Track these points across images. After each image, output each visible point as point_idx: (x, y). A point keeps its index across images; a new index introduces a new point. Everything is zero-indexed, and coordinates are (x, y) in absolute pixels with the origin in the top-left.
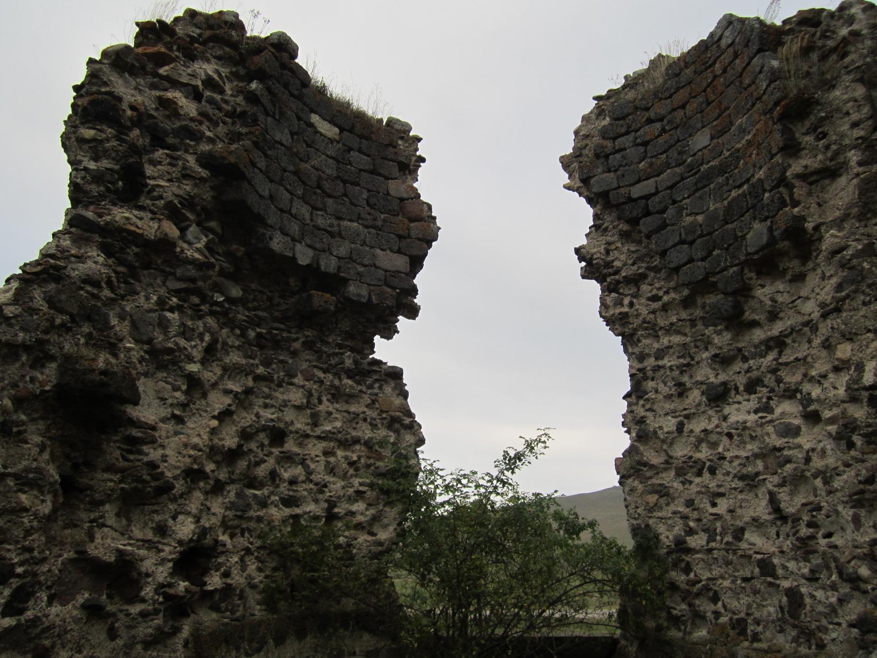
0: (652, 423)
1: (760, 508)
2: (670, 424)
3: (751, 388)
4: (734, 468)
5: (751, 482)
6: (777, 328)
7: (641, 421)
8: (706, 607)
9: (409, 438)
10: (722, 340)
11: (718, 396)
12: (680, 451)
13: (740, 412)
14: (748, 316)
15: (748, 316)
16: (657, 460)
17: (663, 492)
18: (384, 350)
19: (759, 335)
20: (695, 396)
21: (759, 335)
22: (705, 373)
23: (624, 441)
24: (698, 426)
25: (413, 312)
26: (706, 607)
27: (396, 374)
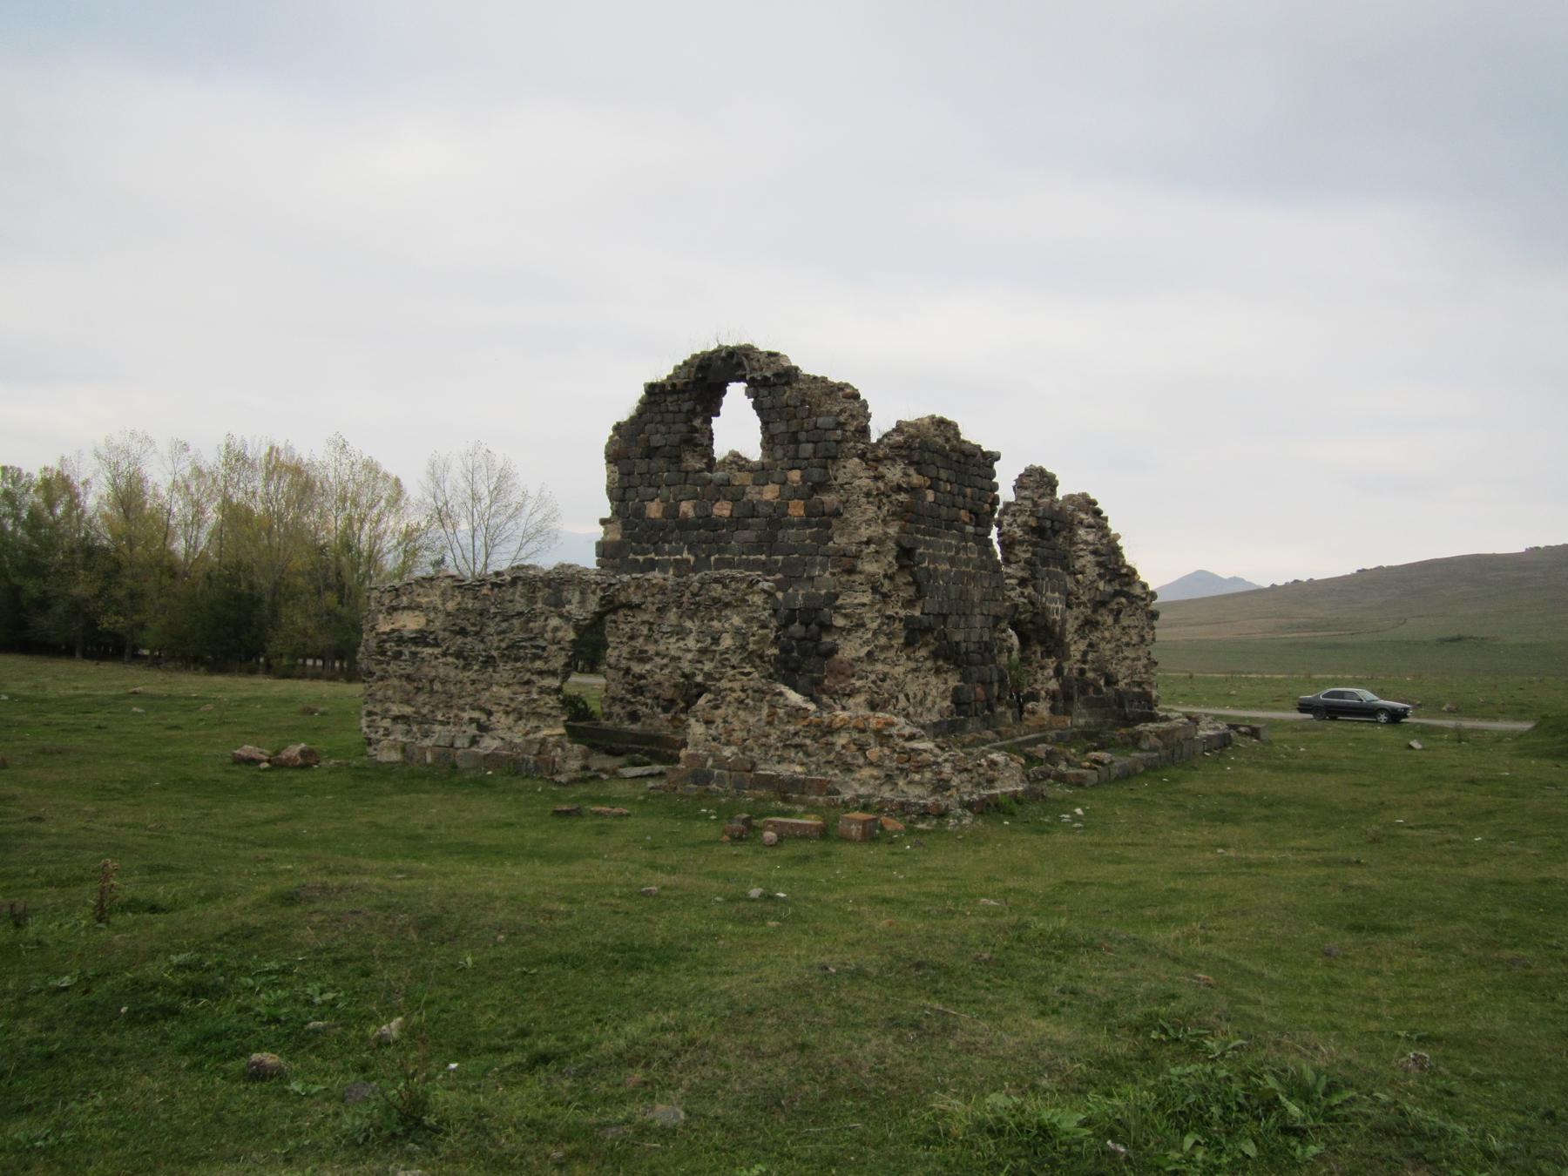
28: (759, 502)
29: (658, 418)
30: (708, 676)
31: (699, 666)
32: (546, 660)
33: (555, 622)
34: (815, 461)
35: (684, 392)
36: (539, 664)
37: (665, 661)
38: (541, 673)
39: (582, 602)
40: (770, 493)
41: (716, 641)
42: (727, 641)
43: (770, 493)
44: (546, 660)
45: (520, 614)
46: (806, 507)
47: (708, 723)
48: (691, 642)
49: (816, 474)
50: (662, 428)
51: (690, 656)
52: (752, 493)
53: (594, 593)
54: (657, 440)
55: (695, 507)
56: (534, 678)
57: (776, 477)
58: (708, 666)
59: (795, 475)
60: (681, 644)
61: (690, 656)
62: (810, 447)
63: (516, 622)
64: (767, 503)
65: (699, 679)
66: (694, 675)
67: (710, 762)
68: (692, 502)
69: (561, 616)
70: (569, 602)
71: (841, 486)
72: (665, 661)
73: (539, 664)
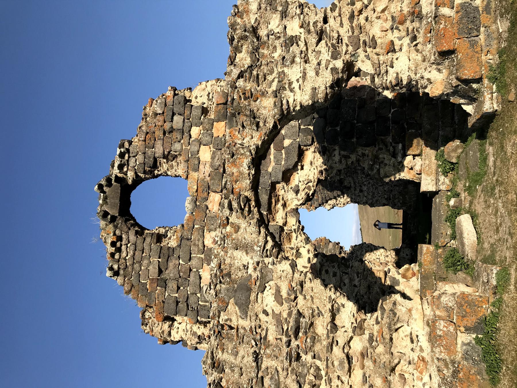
0: (364, 201)
1: (381, 188)
2: (365, 198)
3: (361, 186)
4: (374, 190)
5: (376, 188)
6: (352, 182)
7: (364, 203)
8: (397, 196)
9: (365, 245)
10: (352, 189)
11: (361, 191)
12: (370, 197)
13: (365, 188)
14: (349, 186)
15: (349, 186)
16: (371, 201)
17: (377, 201)
18: (347, 248)
19: (352, 185)
20: (360, 194)
21: (352, 185)
22: (357, 192)
23: (368, 207)
24: (366, 194)
25: (339, 243)
26: (397, 196)
27: (352, 247)
28: (212, 166)
29: (136, 266)
30: (335, 56)
31: (323, 63)
32: (316, 313)
33: (268, 299)
34: (187, 112)
35: (120, 238)
36: (321, 327)
37: (347, 281)
38: (334, 327)
39: (247, 248)
40: (205, 154)
41: (293, 40)
42: (294, 28)
43: (205, 154)
44: (316, 313)
45: (257, 357)
46: (218, 121)
47: (391, 49)
48: (294, 73)
49: (196, 112)
50: (145, 262)
51: (311, 73)
52: (205, 170)
53: (237, 228)
54: (153, 271)
55: (210, 231)
56: (341, 343)
57: (194, 148)
58: (325, 56)
59: (195, 131)
60: (295, 85)
61: (311, 73)
62: (175, 118)
63: (266, 363)
64: (213, 158)
65: (339, 64)
66: (334, 70)
67: (445, 11)
68: (207, 235)
69: (263, 289)
70: (246, 267)
71: (209, 100)
72: (347, 281)
73: (321, 327)
